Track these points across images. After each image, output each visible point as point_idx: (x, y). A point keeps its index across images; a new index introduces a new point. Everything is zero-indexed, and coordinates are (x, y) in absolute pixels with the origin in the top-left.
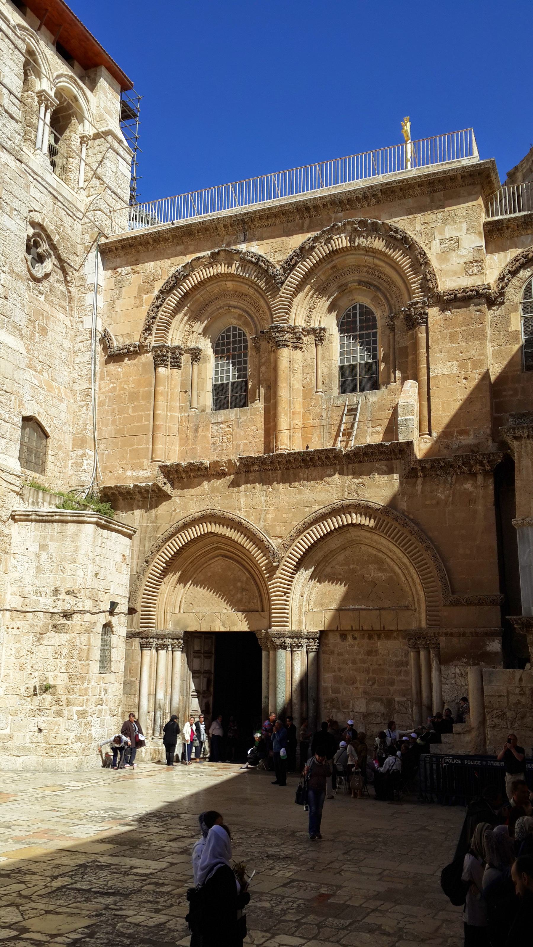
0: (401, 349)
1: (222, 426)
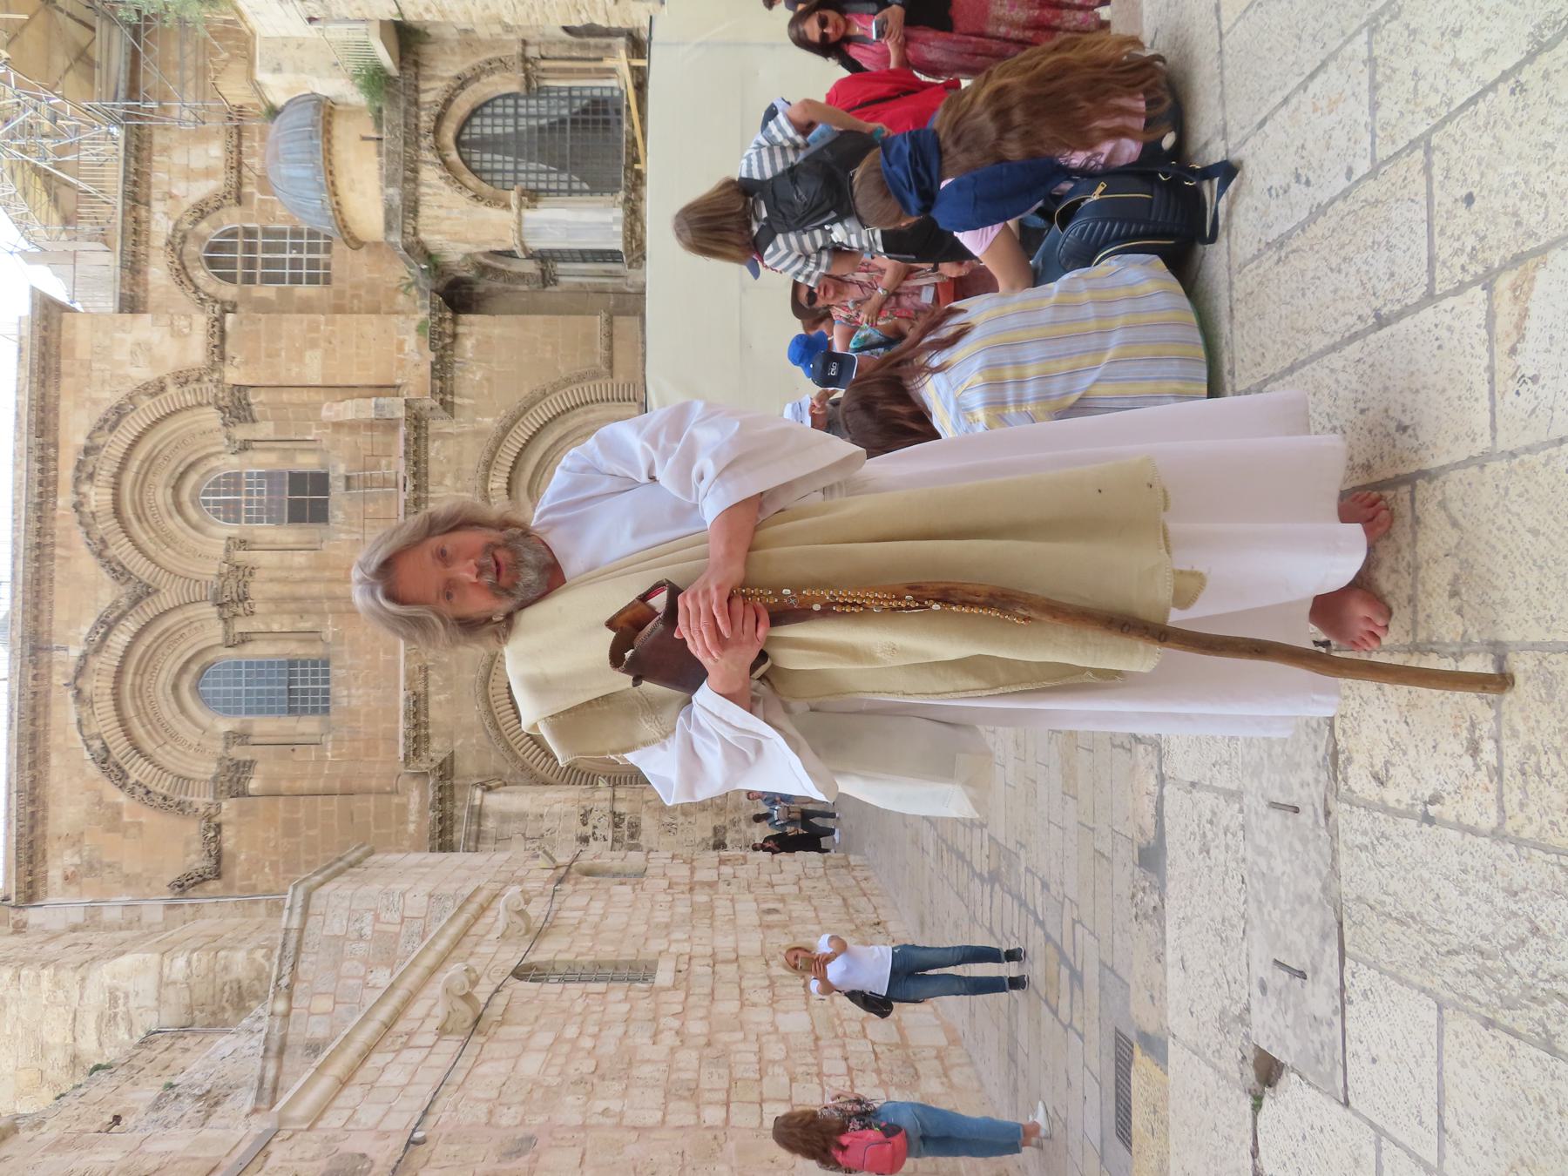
0: (276, 431)
1: (353, 691)
